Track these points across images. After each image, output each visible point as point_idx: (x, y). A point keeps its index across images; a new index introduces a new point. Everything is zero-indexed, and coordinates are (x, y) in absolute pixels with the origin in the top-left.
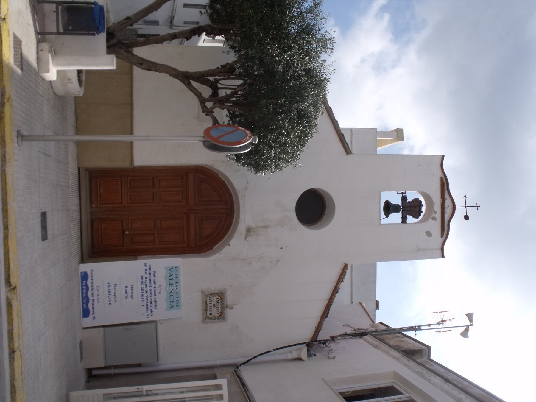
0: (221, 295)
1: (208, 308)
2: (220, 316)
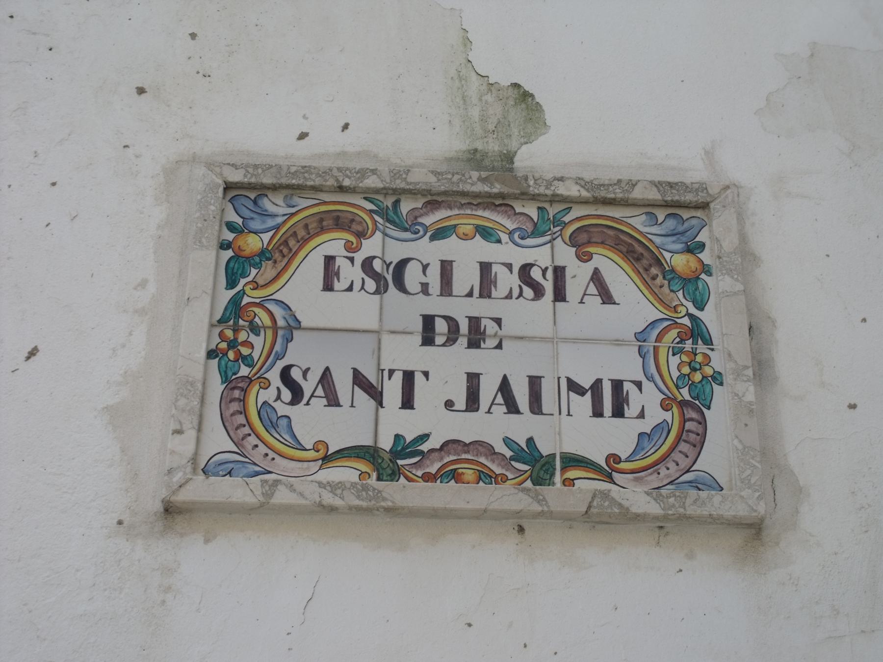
0: (264, 221)
1: (492, 427)
2: (638, 256)
